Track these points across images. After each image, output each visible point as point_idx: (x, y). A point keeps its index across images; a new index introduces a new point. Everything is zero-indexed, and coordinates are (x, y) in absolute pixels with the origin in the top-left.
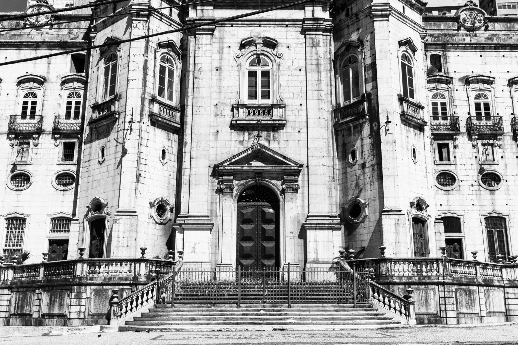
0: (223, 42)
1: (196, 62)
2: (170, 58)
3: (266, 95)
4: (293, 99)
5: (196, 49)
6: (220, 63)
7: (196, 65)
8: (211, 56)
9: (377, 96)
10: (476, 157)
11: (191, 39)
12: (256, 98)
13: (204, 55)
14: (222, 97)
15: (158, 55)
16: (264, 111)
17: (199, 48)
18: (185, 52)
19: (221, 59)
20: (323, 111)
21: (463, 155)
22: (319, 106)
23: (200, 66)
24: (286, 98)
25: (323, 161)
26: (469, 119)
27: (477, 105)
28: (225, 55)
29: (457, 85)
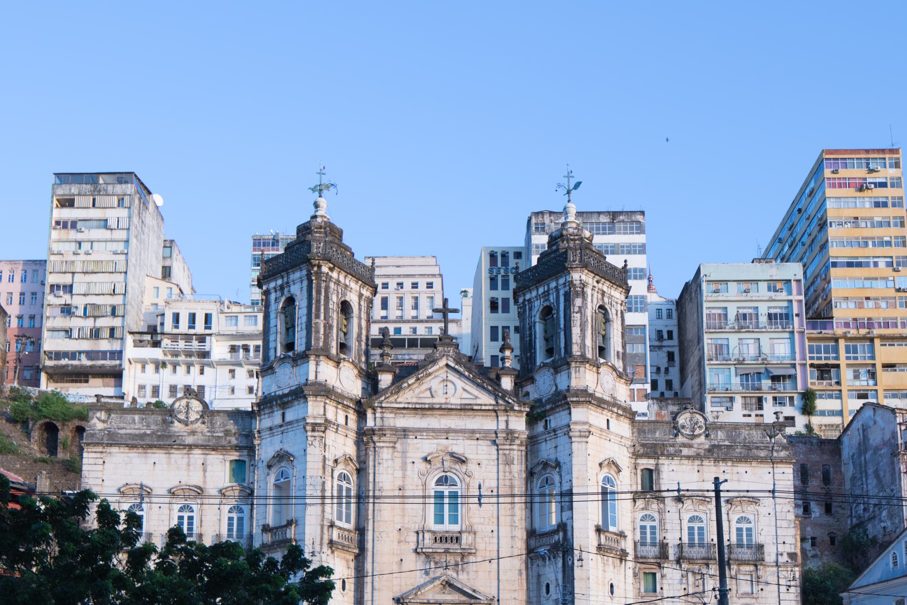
0: (406, 458)
1: (376, 481)
2: (347, 476)
3: (454, 520)
4: (483, 524)
5: (377, 465)
6: (403, 482)
7: (377, 484)
8: (393, 474)
9: (572, 527)
10: (685, 589)
11: (370, 453)
12: (443, 523)
13: (385, 472)
14: (406, 521)
15: (336, 475)
16: (452, 538)
17: (380, 464)
18: (363, 465)
19: (404, 477)
20: (517, 539)
21: (671, 586)
22: (512, 533)
23: (381, 485)
24: (476, 523)
25: (515, 595)
26: (680, 546)
27: (691, 529)
28: (409, 473)
29: (670, 504)
